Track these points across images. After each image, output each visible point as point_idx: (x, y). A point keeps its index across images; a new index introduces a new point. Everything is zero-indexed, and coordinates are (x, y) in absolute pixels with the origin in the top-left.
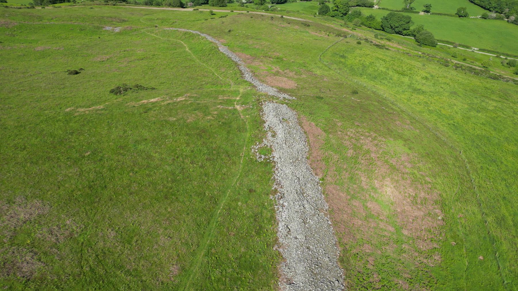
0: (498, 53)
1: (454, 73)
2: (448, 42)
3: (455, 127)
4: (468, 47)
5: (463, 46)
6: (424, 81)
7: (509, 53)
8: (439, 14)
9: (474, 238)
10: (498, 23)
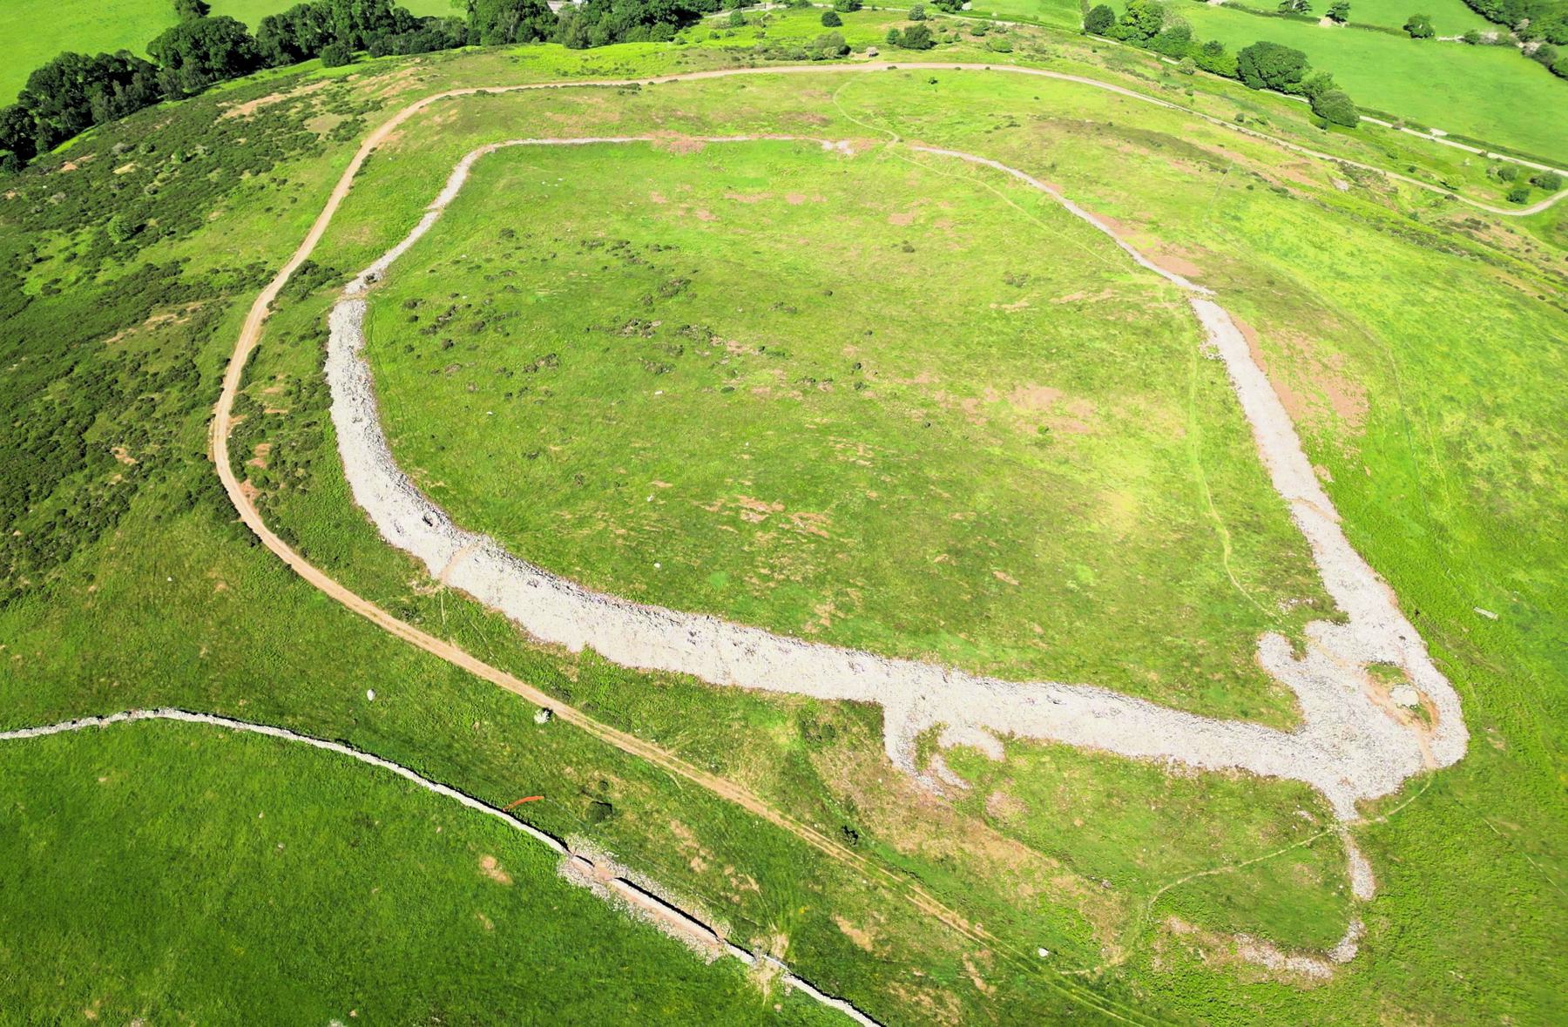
0: (1484, 144)
1: (1389, 242)
2: (1381, 116)
3: (1385, 325)
4: (1423, 129)
5: (1414, 126)
6: (1349, 259)
7: (1508, 146)
8: (1366, 27)
9: (1393, 421)
10: (1501, 55)
